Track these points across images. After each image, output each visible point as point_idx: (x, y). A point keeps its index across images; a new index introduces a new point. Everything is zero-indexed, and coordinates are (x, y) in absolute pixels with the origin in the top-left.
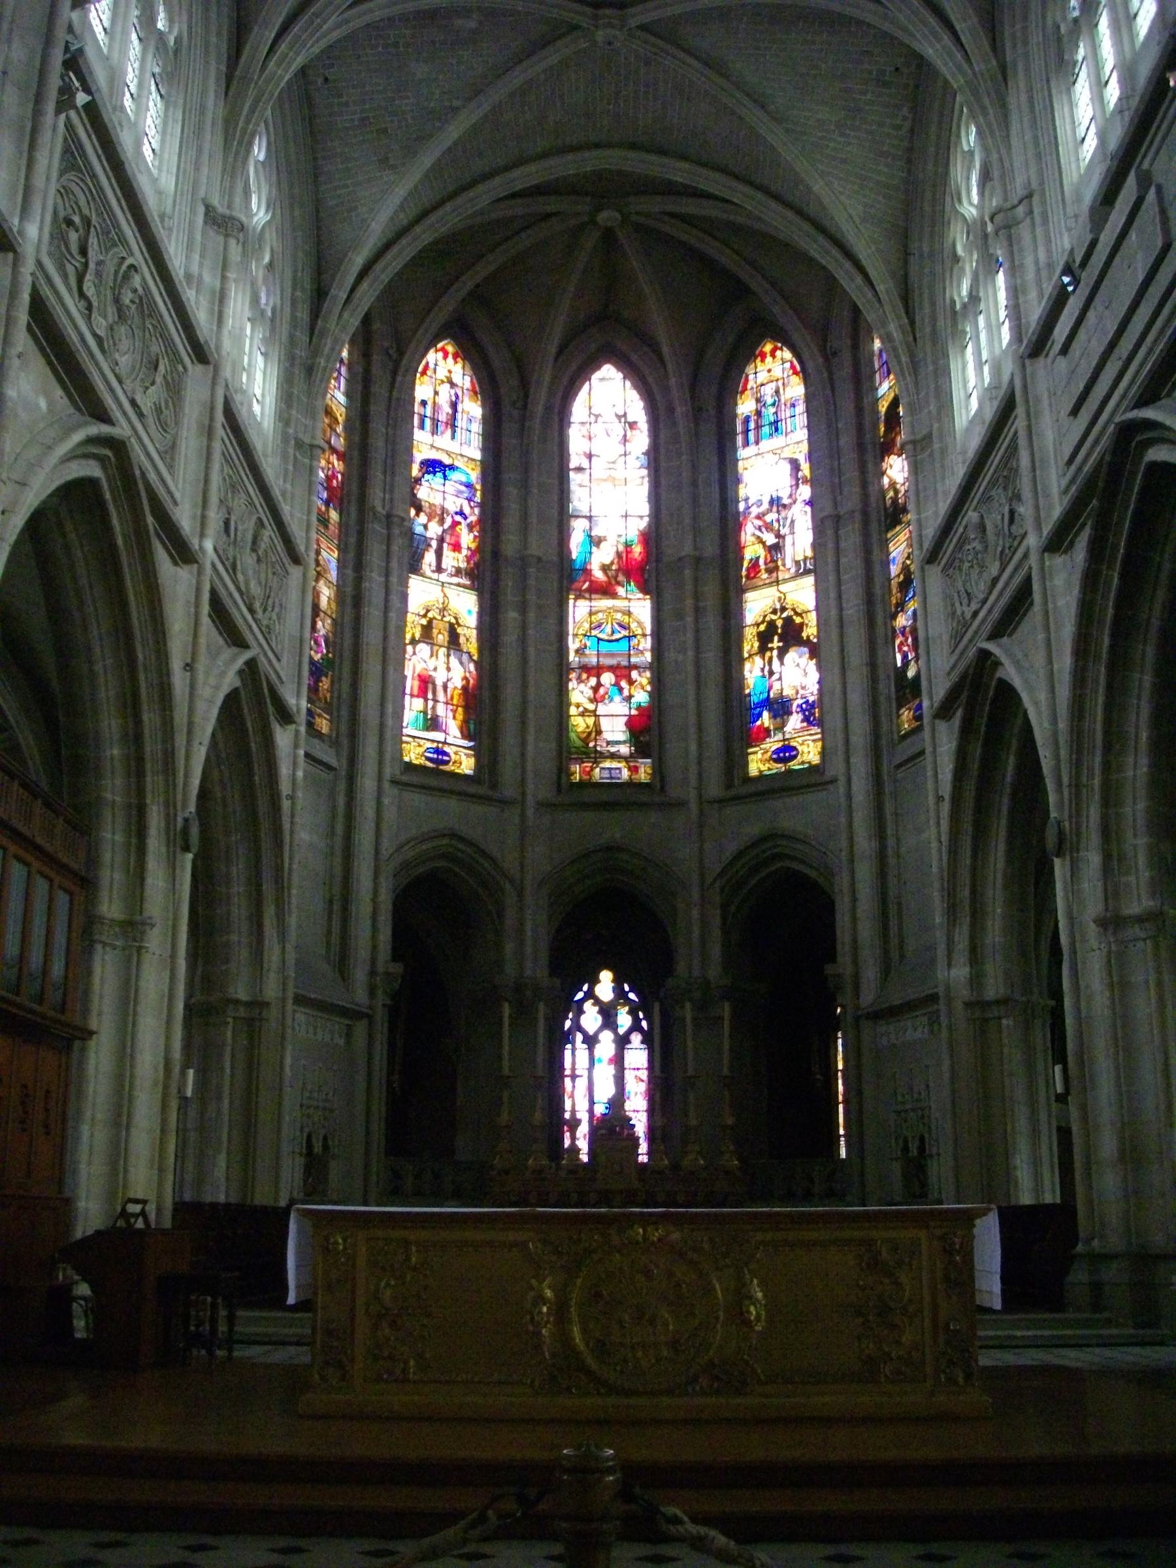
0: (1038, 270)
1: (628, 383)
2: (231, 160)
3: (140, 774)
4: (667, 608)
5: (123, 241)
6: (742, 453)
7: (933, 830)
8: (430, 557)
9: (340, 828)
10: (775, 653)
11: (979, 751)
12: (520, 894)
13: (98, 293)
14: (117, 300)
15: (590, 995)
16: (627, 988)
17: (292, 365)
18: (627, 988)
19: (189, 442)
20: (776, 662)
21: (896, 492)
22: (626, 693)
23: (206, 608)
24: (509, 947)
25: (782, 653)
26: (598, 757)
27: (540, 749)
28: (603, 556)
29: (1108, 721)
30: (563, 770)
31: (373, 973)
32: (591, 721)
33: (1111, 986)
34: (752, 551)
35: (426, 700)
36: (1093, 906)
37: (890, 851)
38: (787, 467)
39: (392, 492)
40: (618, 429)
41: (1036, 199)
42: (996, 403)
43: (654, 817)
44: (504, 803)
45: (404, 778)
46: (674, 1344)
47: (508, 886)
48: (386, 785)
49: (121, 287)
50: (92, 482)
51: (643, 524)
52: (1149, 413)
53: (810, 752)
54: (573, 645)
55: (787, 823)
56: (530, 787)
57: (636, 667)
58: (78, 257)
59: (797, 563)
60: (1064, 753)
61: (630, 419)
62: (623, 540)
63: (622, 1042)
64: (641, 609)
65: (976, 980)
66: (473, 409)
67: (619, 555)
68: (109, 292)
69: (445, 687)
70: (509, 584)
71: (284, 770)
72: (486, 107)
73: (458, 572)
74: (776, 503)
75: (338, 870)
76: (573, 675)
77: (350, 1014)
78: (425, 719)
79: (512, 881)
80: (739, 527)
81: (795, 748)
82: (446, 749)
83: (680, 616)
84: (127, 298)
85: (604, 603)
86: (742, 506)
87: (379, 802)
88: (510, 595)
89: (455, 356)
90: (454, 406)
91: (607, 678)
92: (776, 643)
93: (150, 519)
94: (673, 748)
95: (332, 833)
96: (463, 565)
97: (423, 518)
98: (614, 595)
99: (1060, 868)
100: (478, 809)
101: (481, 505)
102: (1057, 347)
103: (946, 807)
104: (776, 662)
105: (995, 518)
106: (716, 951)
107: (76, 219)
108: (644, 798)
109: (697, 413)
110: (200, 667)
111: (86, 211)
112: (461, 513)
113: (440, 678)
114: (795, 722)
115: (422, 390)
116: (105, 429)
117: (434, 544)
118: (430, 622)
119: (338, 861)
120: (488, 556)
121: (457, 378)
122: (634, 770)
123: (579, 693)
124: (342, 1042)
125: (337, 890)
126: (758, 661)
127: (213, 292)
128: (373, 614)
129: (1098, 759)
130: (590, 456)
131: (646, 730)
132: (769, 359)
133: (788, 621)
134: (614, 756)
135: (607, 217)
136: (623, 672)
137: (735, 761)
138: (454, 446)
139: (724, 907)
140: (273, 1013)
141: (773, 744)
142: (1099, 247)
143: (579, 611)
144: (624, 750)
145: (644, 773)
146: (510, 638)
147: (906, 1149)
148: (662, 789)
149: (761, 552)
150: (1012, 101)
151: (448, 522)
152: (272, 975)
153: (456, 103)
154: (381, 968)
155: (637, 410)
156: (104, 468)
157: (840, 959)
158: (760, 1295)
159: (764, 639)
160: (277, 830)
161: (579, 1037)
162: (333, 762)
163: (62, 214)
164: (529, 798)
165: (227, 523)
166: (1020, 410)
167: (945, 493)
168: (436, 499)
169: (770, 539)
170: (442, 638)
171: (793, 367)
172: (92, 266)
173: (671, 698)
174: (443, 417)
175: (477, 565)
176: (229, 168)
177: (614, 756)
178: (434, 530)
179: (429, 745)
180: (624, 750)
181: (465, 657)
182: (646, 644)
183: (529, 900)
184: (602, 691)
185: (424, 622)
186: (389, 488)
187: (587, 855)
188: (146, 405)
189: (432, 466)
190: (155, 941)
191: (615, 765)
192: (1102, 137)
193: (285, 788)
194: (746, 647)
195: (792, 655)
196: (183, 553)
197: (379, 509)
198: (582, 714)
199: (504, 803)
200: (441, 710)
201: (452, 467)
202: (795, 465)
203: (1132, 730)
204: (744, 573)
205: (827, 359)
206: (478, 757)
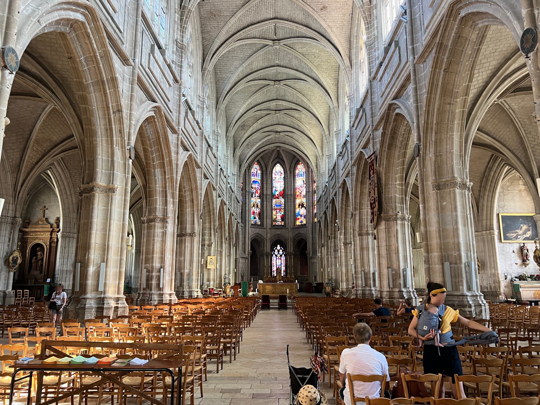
4: (286, 201)
8: (254, 195)
12: (267, 241)
24: (265, 248)
25: (301, 208)
26: (276, 221)
27: (269, 221)
28: (277, 193)
30: (272, 224)
34: (298, 193)
36: (326, 253)
40: (279, 174)
43: (284, 230)
48: (250, 228)
51: (283, 188)
53: (304, 222)
54: (273, 206)
55: (301, 232)
63: (281, 256)
64: (283, 200)
65: (321, 255)
66: (259, 172)
74: (301, 186)
77: (246, 258)
83: (288, 202)
85: (277, 200)
88: (265, 200)
91: (278, 210)
92: (300, 207)
94: (287, 221)
98: (279, 199)
99: (323, 248)
100: (261, 230)
106: (292, 248)
109: (290, 172)
115: (252, 171)
122: (281, 223)
123: (274, 212)
128: (247, 205)
131: (283, 218)
136: (280, 210)
137: (295, 223)
138: (257, 178)
140: (238, 260)
141: (300, 220)
143: (274, 201)
144: (280, 220)
146: (265, 206)
149: (299, 193)
155: (282, 171)
159: (299, 206)
168: (255, 186)
169: (300, 192)
170: (256, 206)
173: (287, 214)
174: (255, 174)
178: (254, 191)
180: (280, 220)
182: (283, 205)
186: (249, 187)
187: (275, 235)
189: (254, 182)
195: (303, 208)
201: (257, 181)
202: (304, 182)
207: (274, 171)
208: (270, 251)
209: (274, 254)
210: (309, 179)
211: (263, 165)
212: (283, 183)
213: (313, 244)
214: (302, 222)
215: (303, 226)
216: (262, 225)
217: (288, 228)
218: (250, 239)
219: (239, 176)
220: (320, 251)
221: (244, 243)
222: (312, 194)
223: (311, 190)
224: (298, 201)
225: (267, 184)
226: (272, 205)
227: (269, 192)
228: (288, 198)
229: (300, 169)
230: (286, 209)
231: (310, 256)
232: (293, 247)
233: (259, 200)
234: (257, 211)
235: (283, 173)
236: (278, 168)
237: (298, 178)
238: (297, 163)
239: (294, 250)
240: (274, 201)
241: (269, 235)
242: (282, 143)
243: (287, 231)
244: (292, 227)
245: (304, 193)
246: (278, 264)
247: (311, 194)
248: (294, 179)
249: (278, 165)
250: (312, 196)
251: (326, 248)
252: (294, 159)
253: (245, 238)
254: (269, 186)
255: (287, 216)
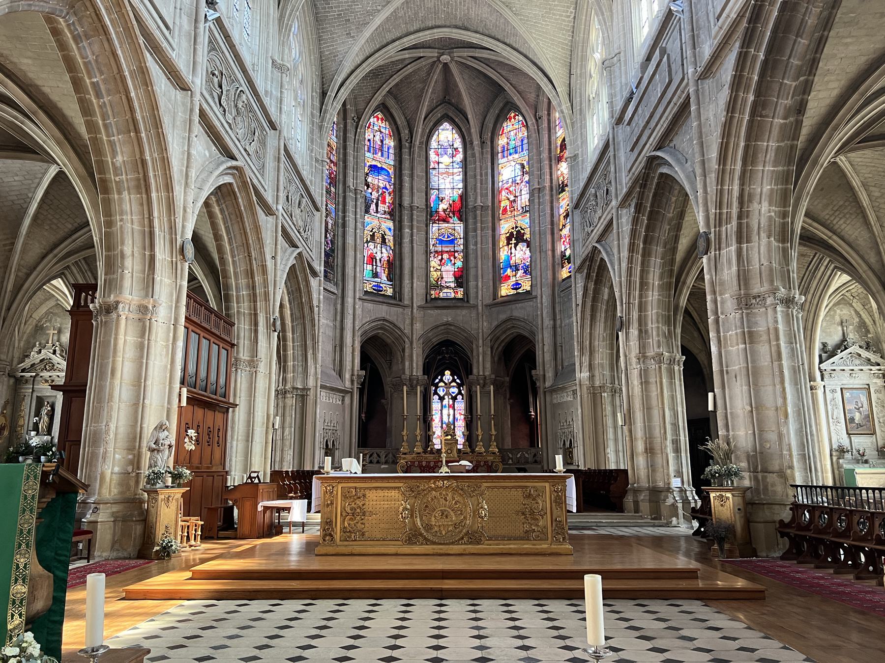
0: (622, 87)
1: (454, 131)
2: (282, 38)
3: (255, 301)
4: (470, 227)
5: (238, 80)
6: (501, 161)
7: (574, 318)
8: (373, 206)
9: (338, 318)
10: (513, 245)
11: (593, 286)
12: (412, 343)
13: (228, 104)
14: (236, 106)
15: (441, 380)
16: (456, 377)
17: (313, 125)
18: (456, 377)
19: (270, 164)
20: (513, 249)
21: (564, 178)
22: (453, 262)
23: (280, 233)
24: (407, 364)
25: (516, 245)
27: (419, 286)
28: (443, 206)
29: (642, 278)
31: (353, 375)
32: (439, 273)
33: (641, 383)
35: (373, 265)
37: (558, 326)
38: (518, 167)
39: (357, 180)
40: (450, 151)
41: (622, 54)
42: (603, 141)
43: (464, 312)
44: (405, 306)
45: (364, 297)
46: (455, 526)
47: (406, 340)
48: (357, 300)
49: (237, 100)
50: (230, 184)
51: (460, 192)
52: (659, 153)
53: (526, 286)
54: (432, 242)
56: (415, 300)
57: (457, 252)
58: (218, 89)
59: (522, 208)
60: (624, 290)
61: (455, 146)
62: (452, 198)
63: (454, 399)
64: (459, 228)
65: (592, 377)
66: (390, 143)
67: (450, 205)
68: (232, 103)
69: (380, 260)
70: (406, 218)
71: (315, 296)
72: (392, 10)
73: (385, 212)
74: (514, 182)
75: (338, 335)
76: (432, 255)
78: (373, 274)
79: (408, 338)
80: (500, 192)
81: (520, 284)
82: (381, 285)
83: (475, 230)
84: (240, 105)
86: (500, 184)
87: (354, 308)
88: (406, 223)
89: (382, 119)
90: (382, 141)
91: (445, 256)
92: (513, 241)
93: (255, 198)
94: (472, 284)
95: (336, 320)
96: (387, 210)
97: (370, 190)
98: (448, 222)
100: (394, 309)
101: (394, 184)
102: (626, 123)
103: (580, 308)
104: (513, 249)
105: (601, 193)
106: (488, 365)
107: (216, 72)
108: (460, 304)
110: (279, 258)
111: (220, 68)
112: (385, 188)
113: (378, 256)
114: (520, 272)
115: (369, 135)
116: (234, 163)
117: (375, 201)
118: (374, 234)
119: (338, 331)
120: (397, 205)
121: (383, 130)
123: (434, 262)
124: (340, 403)
125: (338, 343)
126: (506, 248)
127: (277, 99)
128: (350, 230)
129: (637, 293)
130: (438, 163)
131: (461, 277)
132: (513, 120)
133: (518, 232)
134: (448, 287)
135: (445, 58)
136: (452, 254)
139: (492, 348)
142: (644, 80)
143: (434, 228)
144: (452, 285)
145: (460, 296)
146: (406, 240)
147: (564, 444)
148: (468, 301)
149: (508, 203)
150: (614, 7)
151: (380, 191)
152: (311, 378)
153: (379, 8)
154: (356, 373)
156: (234, 178)
157: (537, 368)
158: (486, 507)
159: (509, 239)
160: (313, 320)
161: (436, 397)
162: (336, 292)
163: (210, 70)
164: (415, 305)
165: (287, 197)
166: (611, 148)
167: (583, 179)
169: (512, 198)
170: (379, 240)
171: (523, 123)
172: (224, 92)
173: (472, 264)
175: (392, 209)
176: (281, 42)
177: (448, 287)
178: (375, 195)
179: (374, 284)
180: (452, 285)
181: (388, 248)
183: (415, 345)
184: (443, 261)
185: (371, 233)
186: (356, 178)
187: (437, 327)
188: (251, 150)
189: (373, 168)
190: (262, 368)
191: (449, 291)
192: (650, 27)
193: (315, 303)
194: (501, 244)
195: (520, 245)
196: (269, 211)
197: (352, 187)
198: (436, 271)
199: (405, 306)
200: (378, 270)
201: (382, 169)
202: (523, 167)
203: (651, 281)
204: (501, 212)
205: (537, 120)
206: (394, 290)
207: (434, 144)
208: (420, 373)
209: (436, 393)
210: (539, 153)
211: (401, 120)
212: (461, 177)
213: (555, 344)
214: (517, 286)
215: (519, 298)
216: (397, 298)
217: (475, 307)
218: (358, 334)
219: (321, 127)
220: (586, 364)
221: (340, 346)
222: (552, 196)
223: (547, 184)
224: (505, 227)
225: (412, 176)
226: (427, 239)
227: (419, 201)
228: (475, 218)
229: (512, 133)
230: (471, 252)
231: (548, 384)
232: (493, 362)
233: (390, 224)
234: (383, 254)
235: (461, 150)
236: (446, 134)
237: (505, 160)
238: (502, 117)
239: (493, 371)
240: (434, 228)
241: (418, 326)
242: (456, 27)
243: (474, 315)
244: (488, 301)
245: (524, 199)
246: (445, 419)
247: (548, 198)
248: (493, 164)
249: (446, 125)
250: (552, 202)
251: (634, 332)
252: (496, 96)
253: (342, 329)
254: (419, 184)
255: (472, 272)
